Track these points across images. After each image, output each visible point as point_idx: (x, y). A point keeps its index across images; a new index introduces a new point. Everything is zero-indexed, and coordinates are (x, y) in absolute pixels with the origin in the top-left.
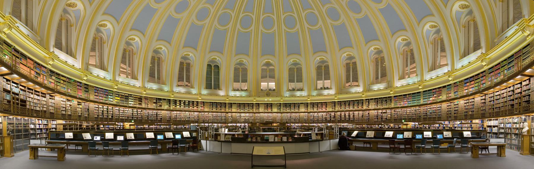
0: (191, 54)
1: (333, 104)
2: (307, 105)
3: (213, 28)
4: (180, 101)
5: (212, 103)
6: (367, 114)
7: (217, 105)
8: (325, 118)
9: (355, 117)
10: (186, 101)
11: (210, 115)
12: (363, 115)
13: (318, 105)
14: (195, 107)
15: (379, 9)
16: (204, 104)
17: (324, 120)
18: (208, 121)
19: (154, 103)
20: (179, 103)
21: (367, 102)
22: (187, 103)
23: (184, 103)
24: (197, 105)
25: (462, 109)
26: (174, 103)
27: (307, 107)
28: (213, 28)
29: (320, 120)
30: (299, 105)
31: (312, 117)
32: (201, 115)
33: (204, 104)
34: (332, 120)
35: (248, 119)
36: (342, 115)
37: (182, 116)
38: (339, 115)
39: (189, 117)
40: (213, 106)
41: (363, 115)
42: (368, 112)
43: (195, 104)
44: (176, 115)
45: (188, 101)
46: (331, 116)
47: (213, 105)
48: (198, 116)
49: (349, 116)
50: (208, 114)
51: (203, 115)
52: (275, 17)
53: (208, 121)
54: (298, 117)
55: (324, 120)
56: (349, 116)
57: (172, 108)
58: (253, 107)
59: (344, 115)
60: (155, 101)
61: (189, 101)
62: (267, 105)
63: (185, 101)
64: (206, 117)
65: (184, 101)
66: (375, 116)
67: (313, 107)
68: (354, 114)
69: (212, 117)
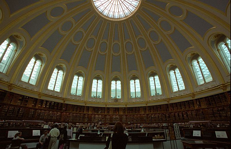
1: (167, 107)
2: (145, 108)
4: (47, 101)
5: (73, 106)
6: (201, 113)
7: (77, 107)
8: (161, 118)
9: (189, 117)
11: (71, 116)
12: (196, 114)
13: (154, 108)
15: (173, 59)
17: (161, 120)
19: (20, 100)
21: (198, 102)
22: (53, 104)
23: (50, 104)
25: (206, 118)
26: (41, 102)
27: (146, 109)
29: (157, 120)
30: (139, 109)
31: (150, 118)
32: (63, 115)
34: (167, 120)
35: (100, 120)
36: (176, 115)
37: (46, 115)
38: (173, 115)
39: (52, 116)
41: (196, 114)
42: (202, 111)
43: (59, 105)
44: (40, 114)
45: (53, 103)
46: (166, 117)
47: (74, 107)
48: (60, 116)
49: (183, 116)
50: (69, 114)
51: (65, 115)
54: (139, 118)
55: (161, 120)
56: (183, 116)
57: (37, 107)
58: (105, 110)
59: (177, 115)
60: (20, 98)
61: (55, 102)
63: (51, 102)
64: (66, 117)
65: (50, 102)
66: (210, 114)
67: (150, 109)
68: (187, 114)
69: (72, 117)
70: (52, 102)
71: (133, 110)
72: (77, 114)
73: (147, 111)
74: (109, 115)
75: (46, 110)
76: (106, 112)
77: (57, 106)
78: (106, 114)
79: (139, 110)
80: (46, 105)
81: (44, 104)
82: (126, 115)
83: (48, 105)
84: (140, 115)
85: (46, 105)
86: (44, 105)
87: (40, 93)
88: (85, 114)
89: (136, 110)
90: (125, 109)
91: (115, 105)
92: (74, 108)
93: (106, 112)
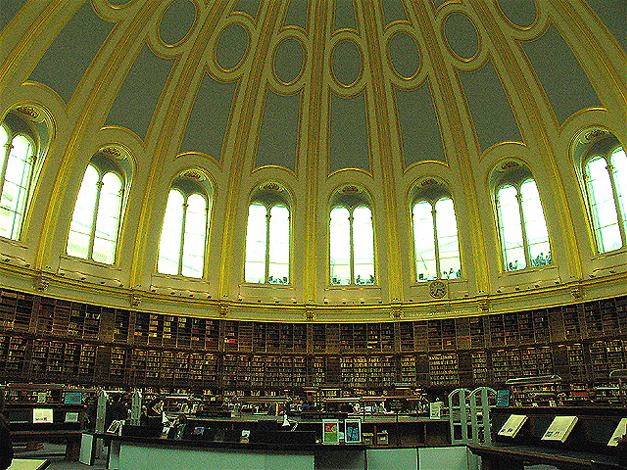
0: (200, 172)
3: (262, 90)
4: (161, 318)
10: (180, 320)
14: (209, 336)
16: (236, 329)
18: (249, 382)
20: (157, 323)
23: (174, 325)
24: (215, 333)
28: (262, 90)
33: (236, 329)
40: (264, 336)
52: (450, 61)
53: (249, 382)
58: (392, 336)
62: (438, 328)
63: (176, 318)
70: (180, 320)
71: (516, 327)
72: (279, 356)
73: (583, 326)
74: (415, 354)
75: (161, 350)
76: (398, 343)
77: (201, 333)
78: (399, 350)
79: (545, 324)
80: (160, 328)
81: (151, 328)
82: (489, 352)
83: (165, 329)
84: (554, 345)
85: (160, 328)
86: (154, 332)
87: (132, 291)
88: (309, 358)
89: (530, 325)
90: (481, 323)
91: (436, 309)
92: (264, 336)
93: (398, 343)
